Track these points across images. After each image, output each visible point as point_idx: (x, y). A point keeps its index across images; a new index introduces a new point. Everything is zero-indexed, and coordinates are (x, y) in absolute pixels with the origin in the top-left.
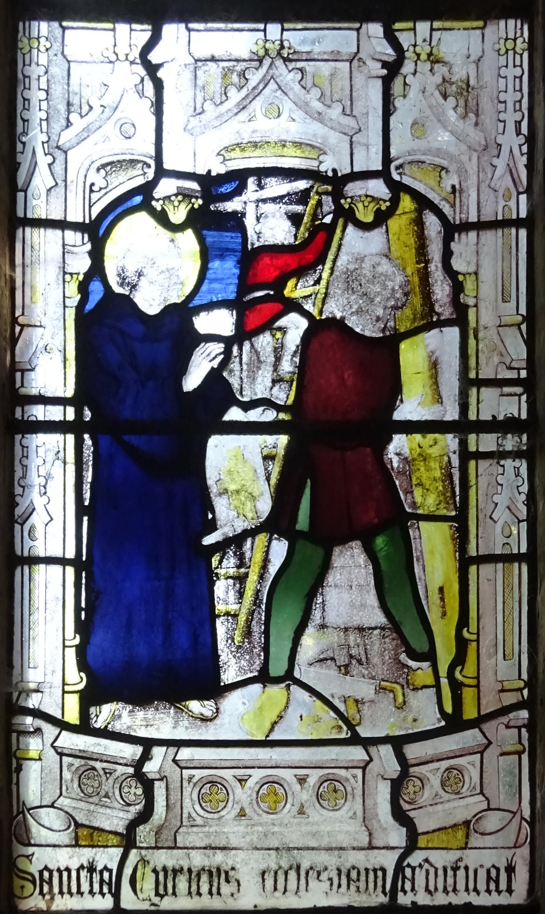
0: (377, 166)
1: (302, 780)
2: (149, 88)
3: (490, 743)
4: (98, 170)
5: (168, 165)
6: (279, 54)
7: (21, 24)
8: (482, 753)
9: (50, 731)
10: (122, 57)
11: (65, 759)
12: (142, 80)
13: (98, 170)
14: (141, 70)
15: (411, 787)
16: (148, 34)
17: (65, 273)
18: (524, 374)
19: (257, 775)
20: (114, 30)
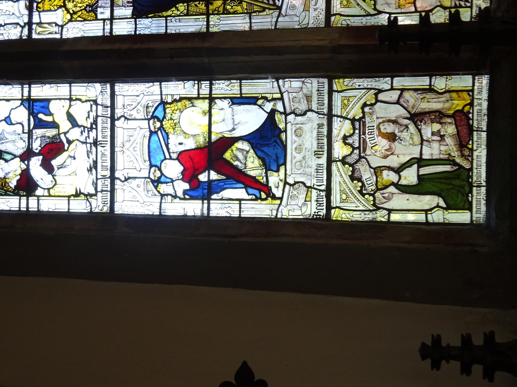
0: (147, 121)
1: (295, 142)
2: (129, 181)
3: (287, 91)
4: (148, 193)
5: (147, 176)
6: (123, 148)
7: (116, 213)
8: (289, 93)
9: (281, 207)
10: (122, 188)
11: (289, 204)
12: (128, 182)
13: (148, 193)
14: (126, 183)
15: (298, 112)
16: (118, 180)
17: (171, 202)
18: (196, 82)
19: (294, 153)
20: (116, 189)
